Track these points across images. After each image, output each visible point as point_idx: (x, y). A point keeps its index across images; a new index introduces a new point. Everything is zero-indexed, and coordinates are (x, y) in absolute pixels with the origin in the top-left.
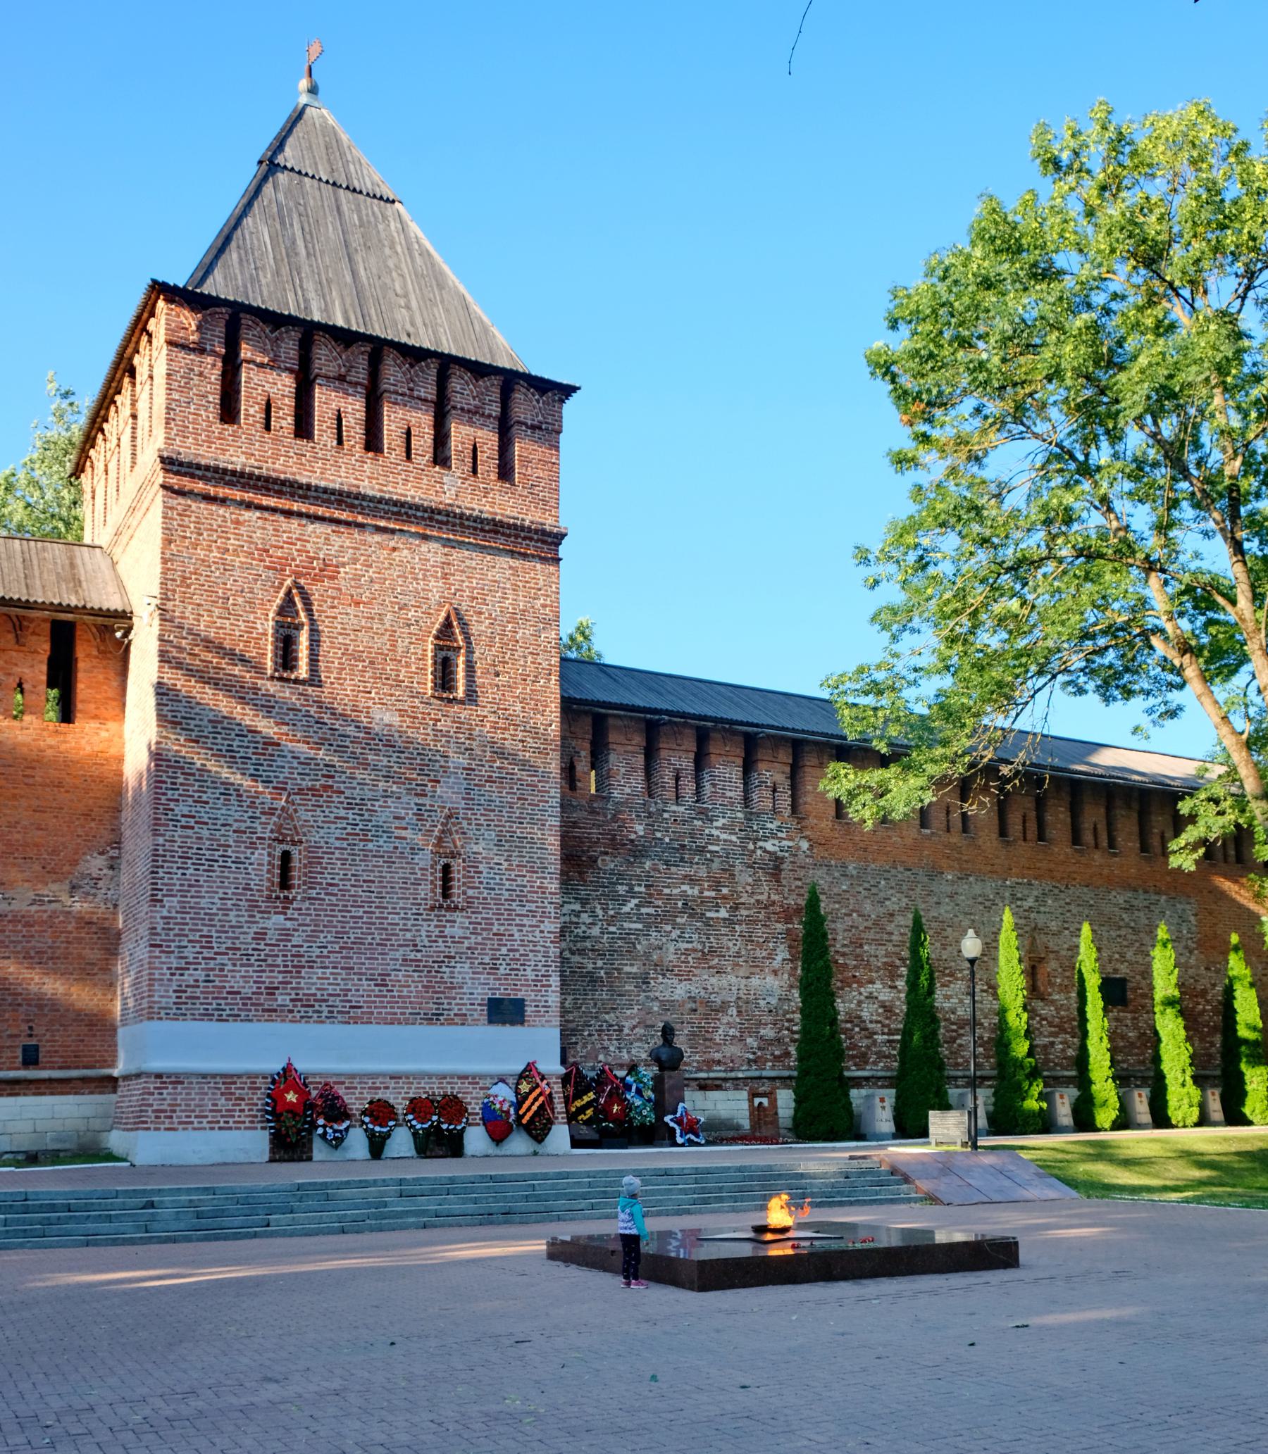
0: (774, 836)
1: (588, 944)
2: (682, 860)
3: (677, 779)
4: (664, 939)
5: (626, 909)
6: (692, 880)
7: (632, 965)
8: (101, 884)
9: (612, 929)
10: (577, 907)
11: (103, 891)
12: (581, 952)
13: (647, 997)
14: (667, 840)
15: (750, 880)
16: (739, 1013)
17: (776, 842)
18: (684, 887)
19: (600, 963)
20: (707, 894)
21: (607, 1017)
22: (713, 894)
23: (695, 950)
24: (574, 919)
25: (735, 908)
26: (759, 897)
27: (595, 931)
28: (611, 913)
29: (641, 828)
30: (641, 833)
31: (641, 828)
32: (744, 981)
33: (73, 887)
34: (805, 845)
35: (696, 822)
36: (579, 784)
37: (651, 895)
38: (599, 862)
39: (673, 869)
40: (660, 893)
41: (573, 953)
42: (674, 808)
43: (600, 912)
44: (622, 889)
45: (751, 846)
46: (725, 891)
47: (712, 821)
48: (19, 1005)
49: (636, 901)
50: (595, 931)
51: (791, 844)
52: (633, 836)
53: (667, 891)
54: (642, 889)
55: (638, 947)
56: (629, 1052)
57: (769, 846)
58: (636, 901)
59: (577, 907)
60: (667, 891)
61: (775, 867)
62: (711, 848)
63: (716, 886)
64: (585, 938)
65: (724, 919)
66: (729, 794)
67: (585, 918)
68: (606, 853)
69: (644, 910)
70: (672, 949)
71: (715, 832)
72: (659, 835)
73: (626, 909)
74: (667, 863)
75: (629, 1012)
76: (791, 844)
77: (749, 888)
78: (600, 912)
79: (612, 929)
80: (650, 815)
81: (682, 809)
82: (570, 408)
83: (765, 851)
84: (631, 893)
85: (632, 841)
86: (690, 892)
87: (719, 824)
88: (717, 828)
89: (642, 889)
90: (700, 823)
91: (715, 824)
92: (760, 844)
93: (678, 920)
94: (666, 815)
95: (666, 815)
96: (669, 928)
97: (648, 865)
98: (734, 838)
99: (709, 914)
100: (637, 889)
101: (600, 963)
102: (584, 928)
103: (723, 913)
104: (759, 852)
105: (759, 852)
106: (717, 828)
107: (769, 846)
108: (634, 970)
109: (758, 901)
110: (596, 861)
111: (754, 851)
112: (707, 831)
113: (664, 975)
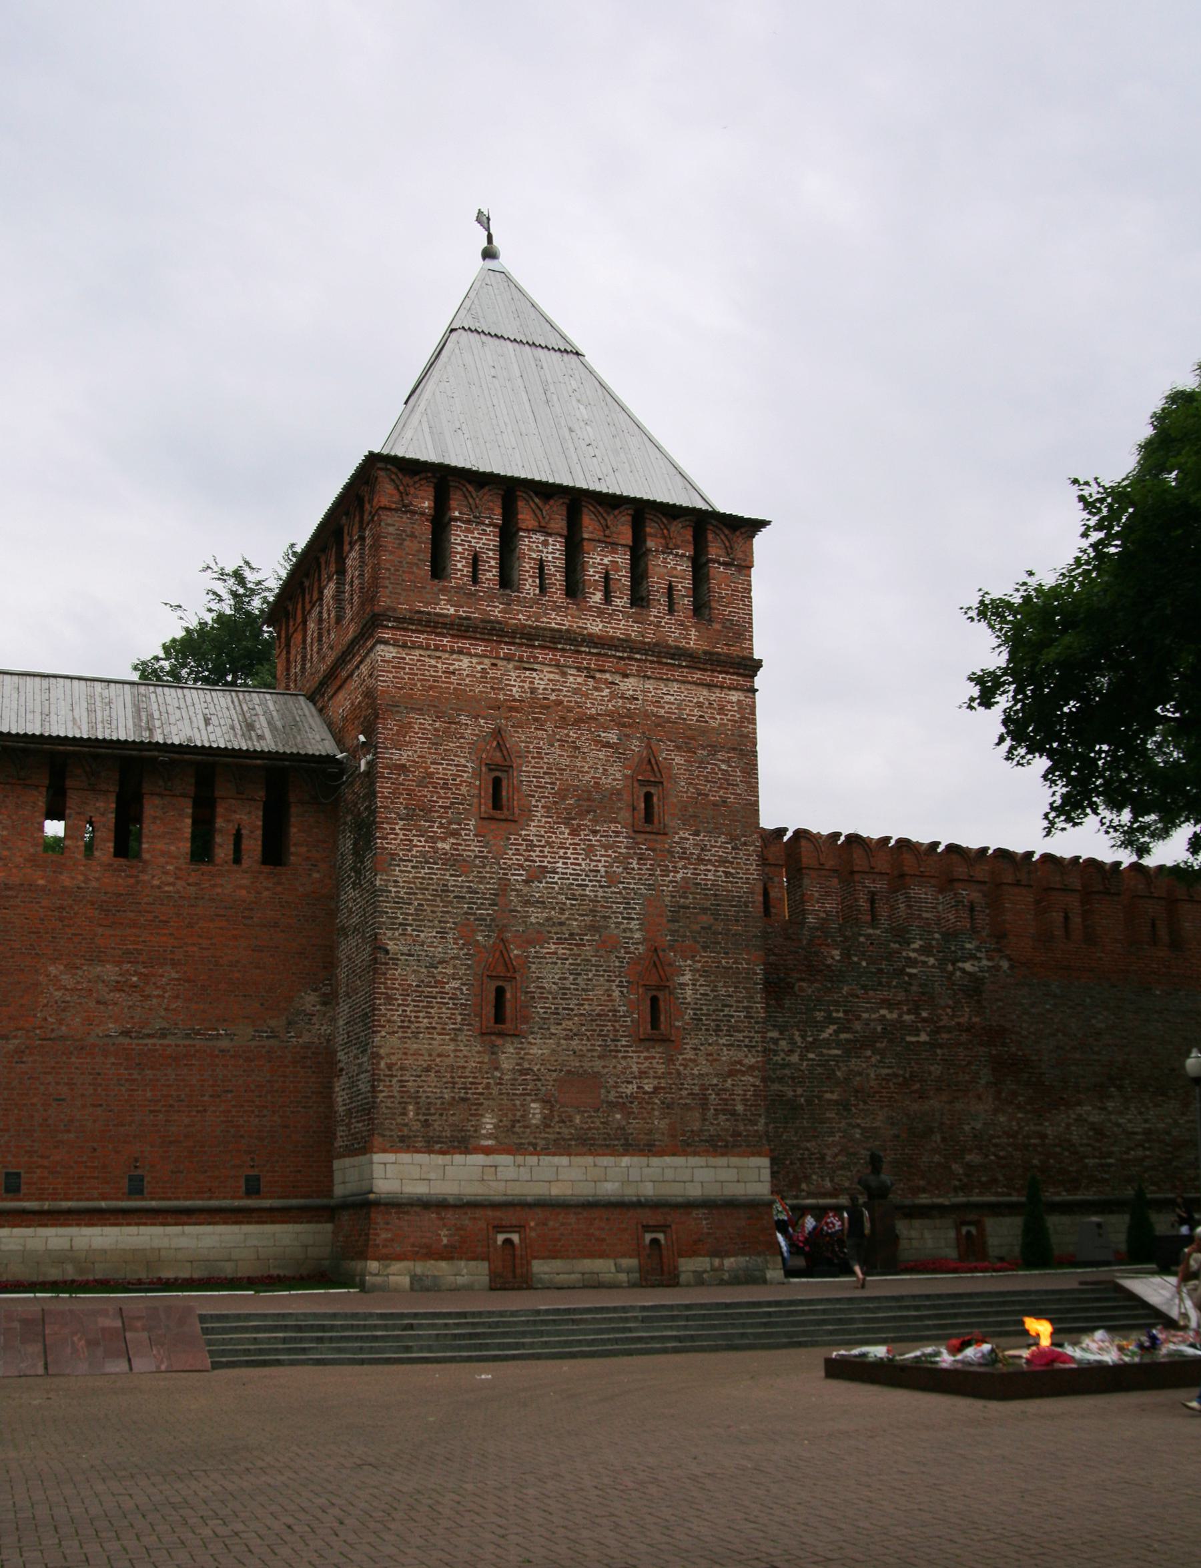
0: (972, 957)
1: (787, 1071)
2: (880, 984)
3: (872, 901)
4: (864, 1065)
5: (825, 1035)
6: (889, 1004)
7: (832, 1092)
8: (314, 1020)
9: (811, 1056)
11: (317, 1027)
12: (780, 1080)
14: (864, 964)
15: (950, 1003)
17: (976, 963)
18: (883, 1012)
19: (799, 1091)
21: (808, 1145)
22: (912, 1017)
23: (896, 1075)
24: (772, 1047)
25: (937, 1031)
26: (960, 1020)
27: (795, 1058)
28: (810, 1039)
29: (838, 952)
30: (838, 958)
31: (838, 952)
33: (289, 1023)
34: (1005, 964)
35: (892, 945)
36: (773, 910)
37: (849, 1021)
38: (796, 988)
39: (871, 993)
40: (859, 1018)
41: (773, 1082)
42: (870, 931)
43: (798, 1039)
44: (819, 1015)
45: (950, 968)
46: (924, 1014)
47: (909, 945)
49: (835, 1027)
50: (795, 1058)
51: (990, 964)
52: (829, 961)
53: (865, 1015)
54: (841, 1015)
55: (839, 1074)
56: (832, 1181)
57: (968, 966)
58: (835, 1027)
60: (865, 1015)
61: (974, 988)
62: (908, 970)
63: (915, 1010)
64: (783, 1066)
65: (925, 1043)
66: (925, 915)
67: (783, 1044)
68: (802, 980)
69: (843, 1036)
70: (872, 1076)
72: (855, 959)
73: (825, 1035)
74: (864, 987)
75: (831, 1139)
77: (949, 1010)
78: (798, 1039)
79: (811, 1056)
80: (846, 939)
81: (878, 932)
82: (760, 541)
83: (963, 971)
84: (830, 1020)
85: (829, 966)
86: (889, 1016)
87: (915, 946)
88: (914, 950)
89: (841, 1015)
90: (897, 946)
92: (960, 965)
93: (878, 1045)
94: (862, 939)
95: (862, 939)
96: (869, 1053)
97: (845, 990)
98: (932, 961)
99: (909, 1039)
100: (835, 1015)
101: (799, 1091)
102: (782, 1055)
103: (924, 1037)
104: (958, 973)
105: (958, 973)
106: (914, 950)
107: (968, 966)
108: (835, 1097)
109: (958, 1024)
110: (792, 988)
111: (952, 973)
112: (904, 954)
113: (865, 1103)
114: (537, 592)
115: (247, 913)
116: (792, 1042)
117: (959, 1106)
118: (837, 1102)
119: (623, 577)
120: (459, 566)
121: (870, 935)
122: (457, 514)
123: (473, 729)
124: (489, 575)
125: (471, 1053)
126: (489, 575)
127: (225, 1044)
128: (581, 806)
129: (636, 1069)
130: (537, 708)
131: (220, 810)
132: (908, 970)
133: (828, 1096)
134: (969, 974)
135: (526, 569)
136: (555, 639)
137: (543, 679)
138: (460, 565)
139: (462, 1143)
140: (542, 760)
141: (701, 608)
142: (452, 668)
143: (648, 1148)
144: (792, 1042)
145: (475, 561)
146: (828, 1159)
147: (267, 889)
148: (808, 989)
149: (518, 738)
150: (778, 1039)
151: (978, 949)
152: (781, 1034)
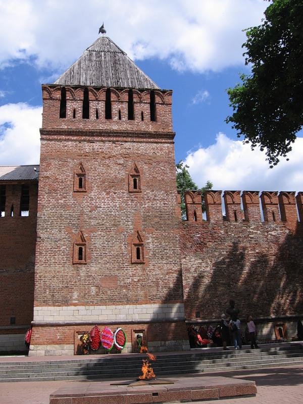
0: (274, 230)
4: (235, 270)
10: (200, 261)
13: (231, 291)
14: (233, 235)
15: (267, 246)
16: (267, 295)
20: (250, 252)
24: (199, 265)
29: (223, 231)
32: (268, 283)
38: (208, 245)
45: (266, 234)
46: (257, 251)
48: (10, 304)
51: (282, 232)
52: (220, 235)
54: (225, 253)
57: (273, 233)
59: (200, 261)
62: (250, 236)
71: (251, 230)
72: (230, 233)
76: (282, 232)
77: (266, 249)
80: (226, 227)
83: (272, 235)
88: (252, 229)
89: (225, 253)
91: (251, 227)
92: (270, 233)
94: (232, 226)
95: (232, 226)
96: (236, 266)
98: (259, 232)
102: (203, 268)
105: (269, 236)
106: (252, 229)
107: (273, 233)
114: (95, 118)
115: (14, 232)
116: (207, 262)
117: (272, 282)
118: (224, 284)
119: (125, 112)
120: (69, 113)
121: (235, 225)
122: (68, 98)
123: (72, 163)
124: (79, 115)
125: (69, 270)
126: (79, 115)
127: (6, 274)
128: (110, 185)
129: (132, 273)
130: (95, 155)
131: (7, 200)
132: (250, 236)
133: (221, 282)
134: (274, 236)
135: (92, 112)
136: (101, 133)
137: (96, 146)
138: (69, 113)
139: (66, 302)
140: (96, 172)
141: (153, 118)
142: (65, 145)
143: (136, 302)
144: (207, 262)
145: (74, 112)
146: (223, 304)
147: (21, 223)
148: (211, 245)
149: (87, 165)
150: (201, 263)
151: (276, 227)
152: (203, 261)
